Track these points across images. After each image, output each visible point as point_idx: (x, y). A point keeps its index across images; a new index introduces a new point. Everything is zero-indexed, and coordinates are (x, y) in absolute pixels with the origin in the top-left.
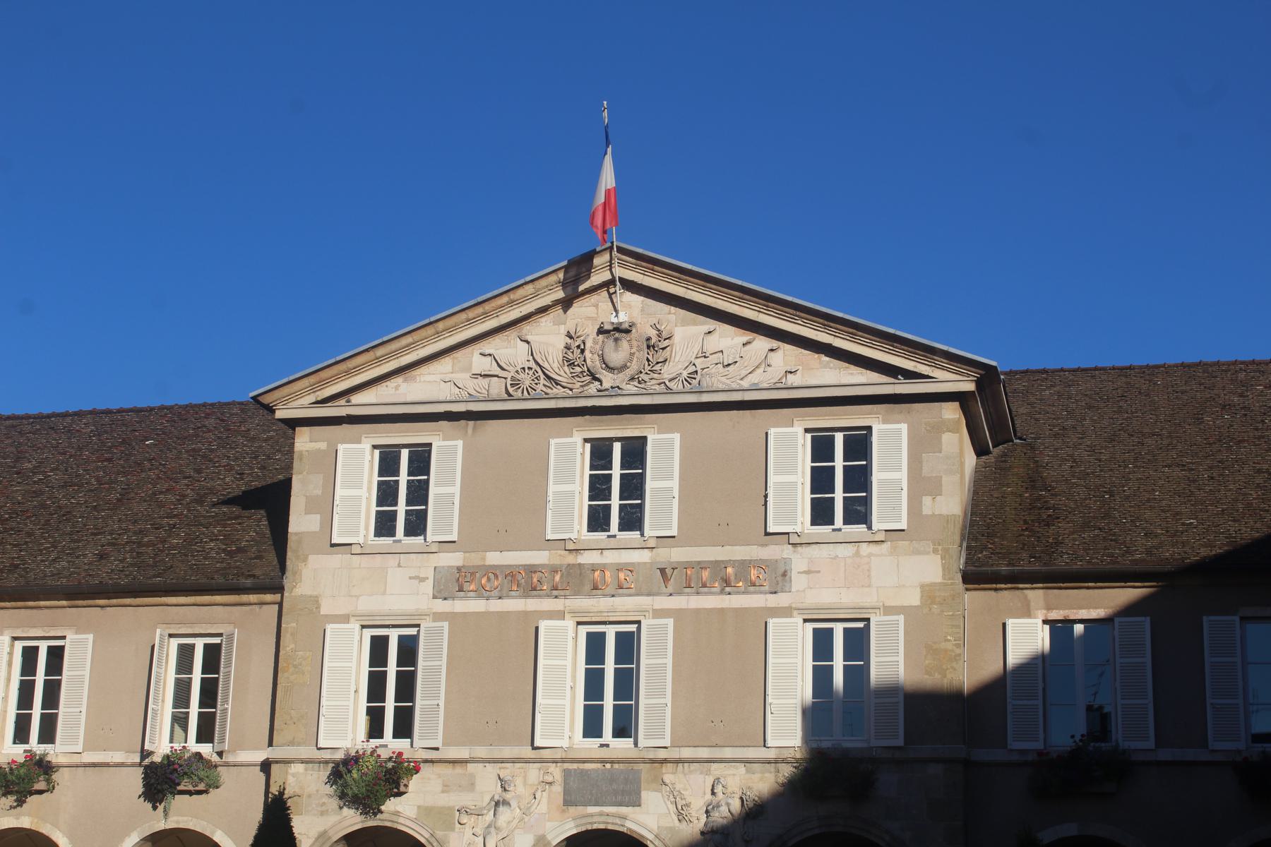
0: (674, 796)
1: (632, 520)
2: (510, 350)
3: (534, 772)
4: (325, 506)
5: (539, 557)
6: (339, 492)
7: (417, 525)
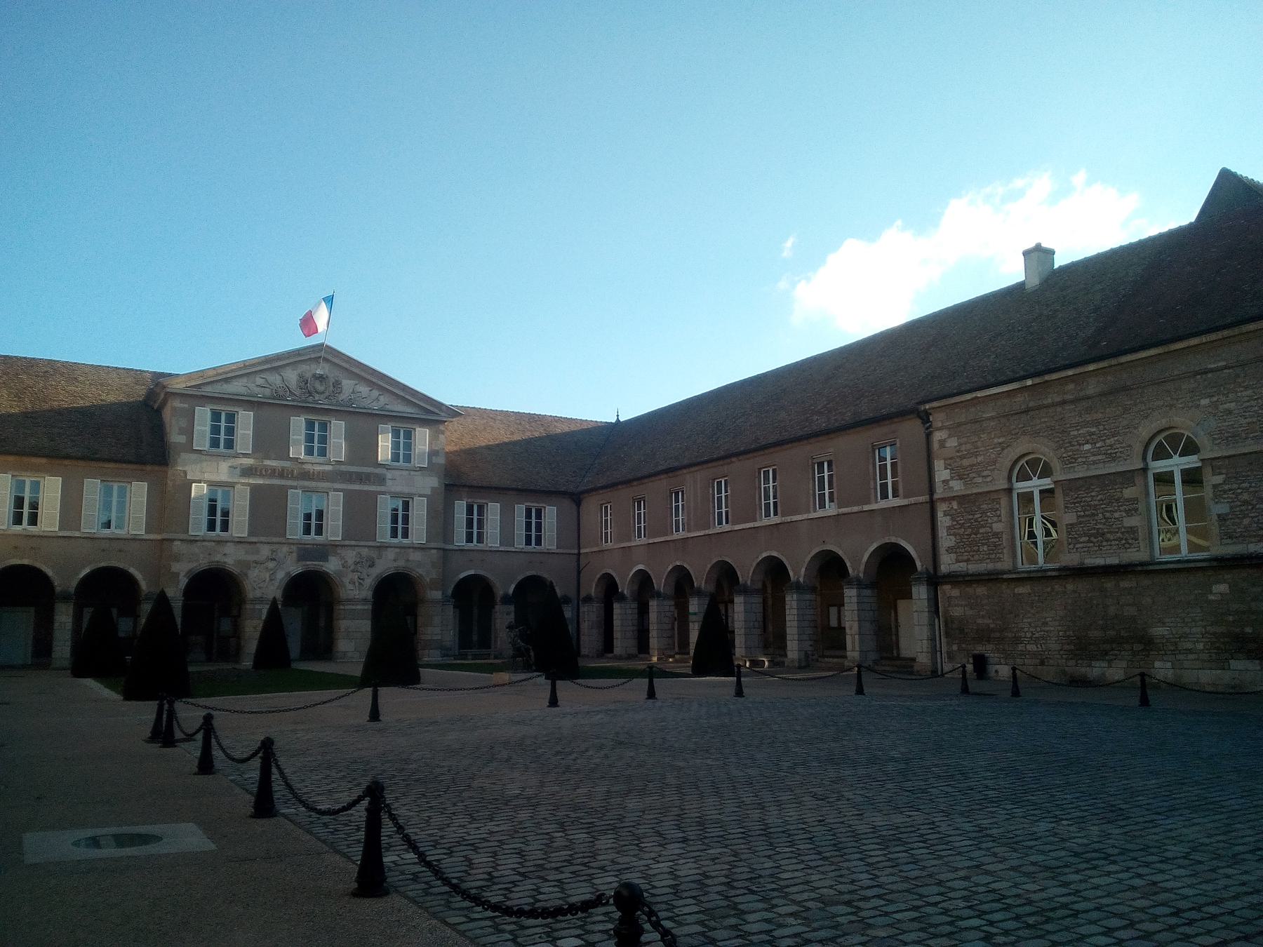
0: (342, 558)
1: (323, 452)
2: (275, 379)
3: (285, 549)
4: (189, 432)
5: (287, 464)
6: (196, 428)
7: (230, 444)
